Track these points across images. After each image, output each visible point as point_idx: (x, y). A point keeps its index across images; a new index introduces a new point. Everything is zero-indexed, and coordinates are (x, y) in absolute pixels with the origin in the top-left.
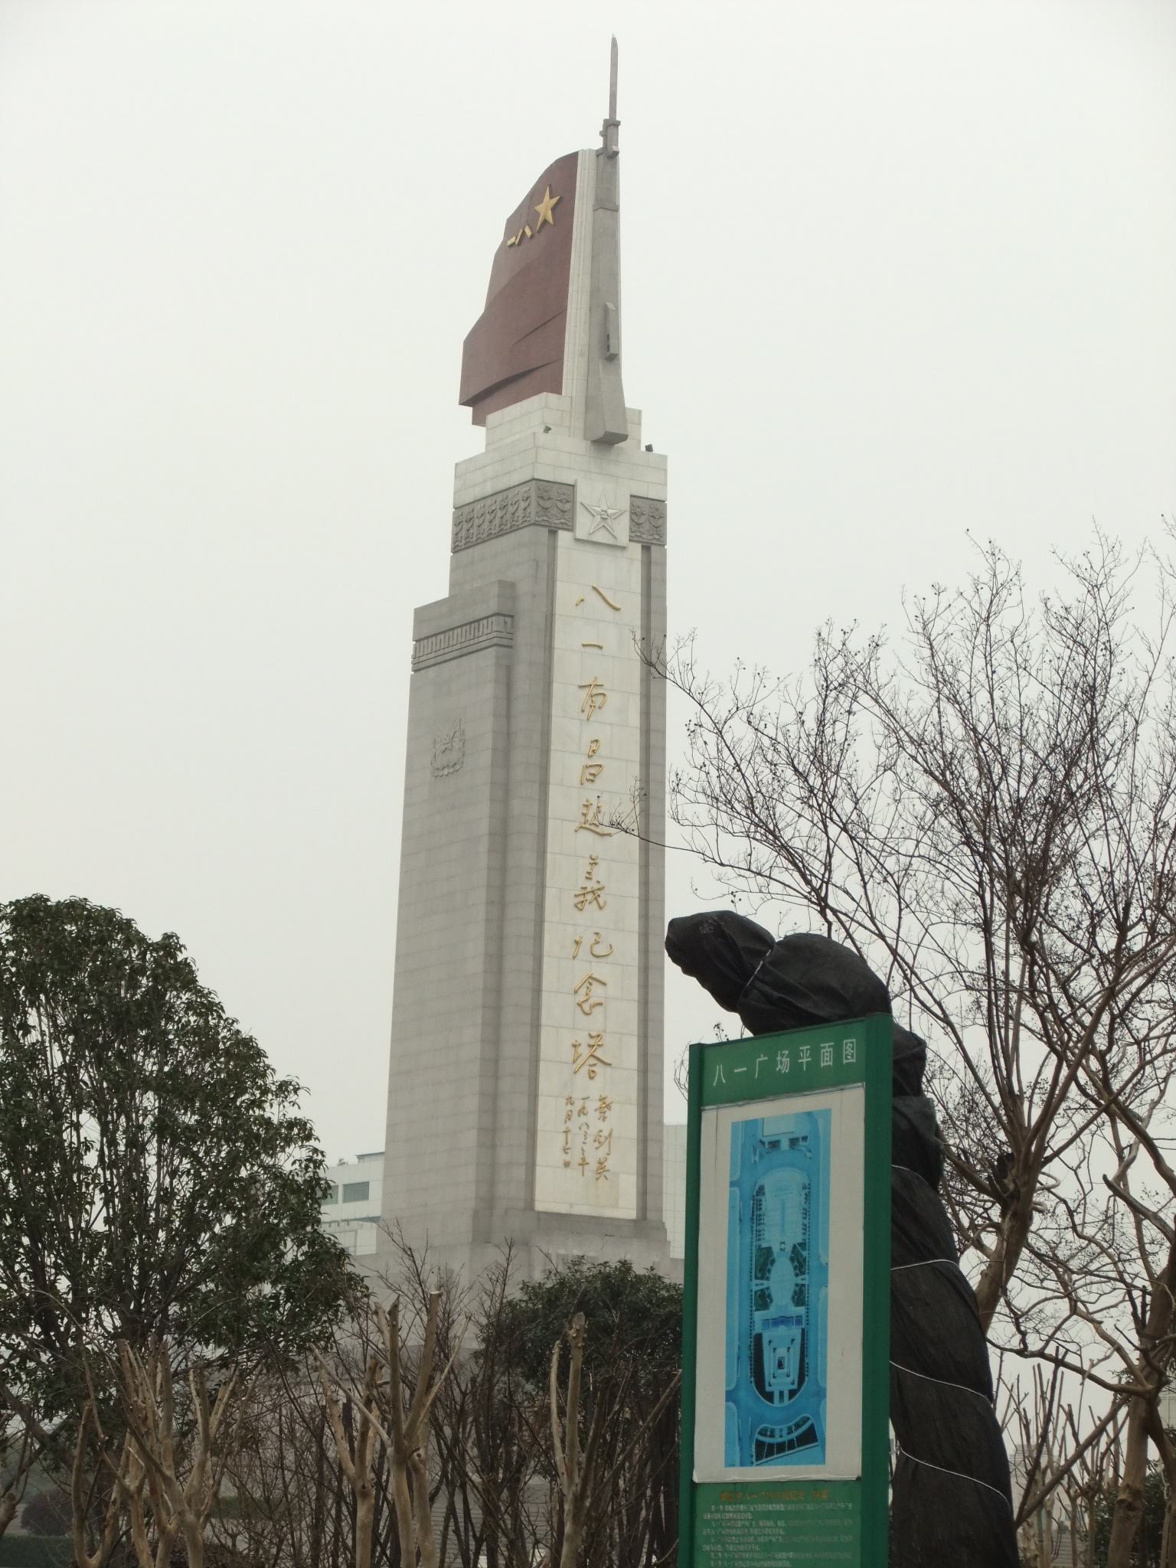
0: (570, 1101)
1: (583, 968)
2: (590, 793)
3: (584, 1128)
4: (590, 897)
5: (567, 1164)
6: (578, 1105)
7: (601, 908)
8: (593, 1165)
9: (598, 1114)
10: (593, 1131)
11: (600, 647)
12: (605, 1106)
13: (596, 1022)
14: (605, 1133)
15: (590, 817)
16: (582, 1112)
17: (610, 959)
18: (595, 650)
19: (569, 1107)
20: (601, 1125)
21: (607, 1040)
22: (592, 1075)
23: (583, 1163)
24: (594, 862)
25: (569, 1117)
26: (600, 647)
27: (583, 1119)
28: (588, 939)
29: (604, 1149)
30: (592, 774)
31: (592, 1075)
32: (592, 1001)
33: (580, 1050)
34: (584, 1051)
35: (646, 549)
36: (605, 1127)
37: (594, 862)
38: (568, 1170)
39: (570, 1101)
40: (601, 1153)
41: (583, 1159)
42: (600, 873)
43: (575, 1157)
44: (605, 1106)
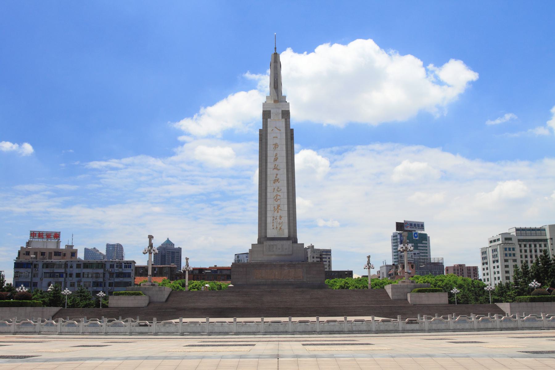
0: (273, 217)
1: (275, 194)
2: (276, 163)
12: (281, 217)
13: (278, 203)
16: (276, 219)
22: (278, 212)
24: (277, 175)
28: (276, 188)
30: (276, 160)
31: (278, 212)
34: (276, 208)
35: (286, 119)
36: (281, 221)
37: (277, 175)
39: (273, 217)
40: (280, 226)
42: (278, 176)
43: (275, 227)
44: (281, 217)
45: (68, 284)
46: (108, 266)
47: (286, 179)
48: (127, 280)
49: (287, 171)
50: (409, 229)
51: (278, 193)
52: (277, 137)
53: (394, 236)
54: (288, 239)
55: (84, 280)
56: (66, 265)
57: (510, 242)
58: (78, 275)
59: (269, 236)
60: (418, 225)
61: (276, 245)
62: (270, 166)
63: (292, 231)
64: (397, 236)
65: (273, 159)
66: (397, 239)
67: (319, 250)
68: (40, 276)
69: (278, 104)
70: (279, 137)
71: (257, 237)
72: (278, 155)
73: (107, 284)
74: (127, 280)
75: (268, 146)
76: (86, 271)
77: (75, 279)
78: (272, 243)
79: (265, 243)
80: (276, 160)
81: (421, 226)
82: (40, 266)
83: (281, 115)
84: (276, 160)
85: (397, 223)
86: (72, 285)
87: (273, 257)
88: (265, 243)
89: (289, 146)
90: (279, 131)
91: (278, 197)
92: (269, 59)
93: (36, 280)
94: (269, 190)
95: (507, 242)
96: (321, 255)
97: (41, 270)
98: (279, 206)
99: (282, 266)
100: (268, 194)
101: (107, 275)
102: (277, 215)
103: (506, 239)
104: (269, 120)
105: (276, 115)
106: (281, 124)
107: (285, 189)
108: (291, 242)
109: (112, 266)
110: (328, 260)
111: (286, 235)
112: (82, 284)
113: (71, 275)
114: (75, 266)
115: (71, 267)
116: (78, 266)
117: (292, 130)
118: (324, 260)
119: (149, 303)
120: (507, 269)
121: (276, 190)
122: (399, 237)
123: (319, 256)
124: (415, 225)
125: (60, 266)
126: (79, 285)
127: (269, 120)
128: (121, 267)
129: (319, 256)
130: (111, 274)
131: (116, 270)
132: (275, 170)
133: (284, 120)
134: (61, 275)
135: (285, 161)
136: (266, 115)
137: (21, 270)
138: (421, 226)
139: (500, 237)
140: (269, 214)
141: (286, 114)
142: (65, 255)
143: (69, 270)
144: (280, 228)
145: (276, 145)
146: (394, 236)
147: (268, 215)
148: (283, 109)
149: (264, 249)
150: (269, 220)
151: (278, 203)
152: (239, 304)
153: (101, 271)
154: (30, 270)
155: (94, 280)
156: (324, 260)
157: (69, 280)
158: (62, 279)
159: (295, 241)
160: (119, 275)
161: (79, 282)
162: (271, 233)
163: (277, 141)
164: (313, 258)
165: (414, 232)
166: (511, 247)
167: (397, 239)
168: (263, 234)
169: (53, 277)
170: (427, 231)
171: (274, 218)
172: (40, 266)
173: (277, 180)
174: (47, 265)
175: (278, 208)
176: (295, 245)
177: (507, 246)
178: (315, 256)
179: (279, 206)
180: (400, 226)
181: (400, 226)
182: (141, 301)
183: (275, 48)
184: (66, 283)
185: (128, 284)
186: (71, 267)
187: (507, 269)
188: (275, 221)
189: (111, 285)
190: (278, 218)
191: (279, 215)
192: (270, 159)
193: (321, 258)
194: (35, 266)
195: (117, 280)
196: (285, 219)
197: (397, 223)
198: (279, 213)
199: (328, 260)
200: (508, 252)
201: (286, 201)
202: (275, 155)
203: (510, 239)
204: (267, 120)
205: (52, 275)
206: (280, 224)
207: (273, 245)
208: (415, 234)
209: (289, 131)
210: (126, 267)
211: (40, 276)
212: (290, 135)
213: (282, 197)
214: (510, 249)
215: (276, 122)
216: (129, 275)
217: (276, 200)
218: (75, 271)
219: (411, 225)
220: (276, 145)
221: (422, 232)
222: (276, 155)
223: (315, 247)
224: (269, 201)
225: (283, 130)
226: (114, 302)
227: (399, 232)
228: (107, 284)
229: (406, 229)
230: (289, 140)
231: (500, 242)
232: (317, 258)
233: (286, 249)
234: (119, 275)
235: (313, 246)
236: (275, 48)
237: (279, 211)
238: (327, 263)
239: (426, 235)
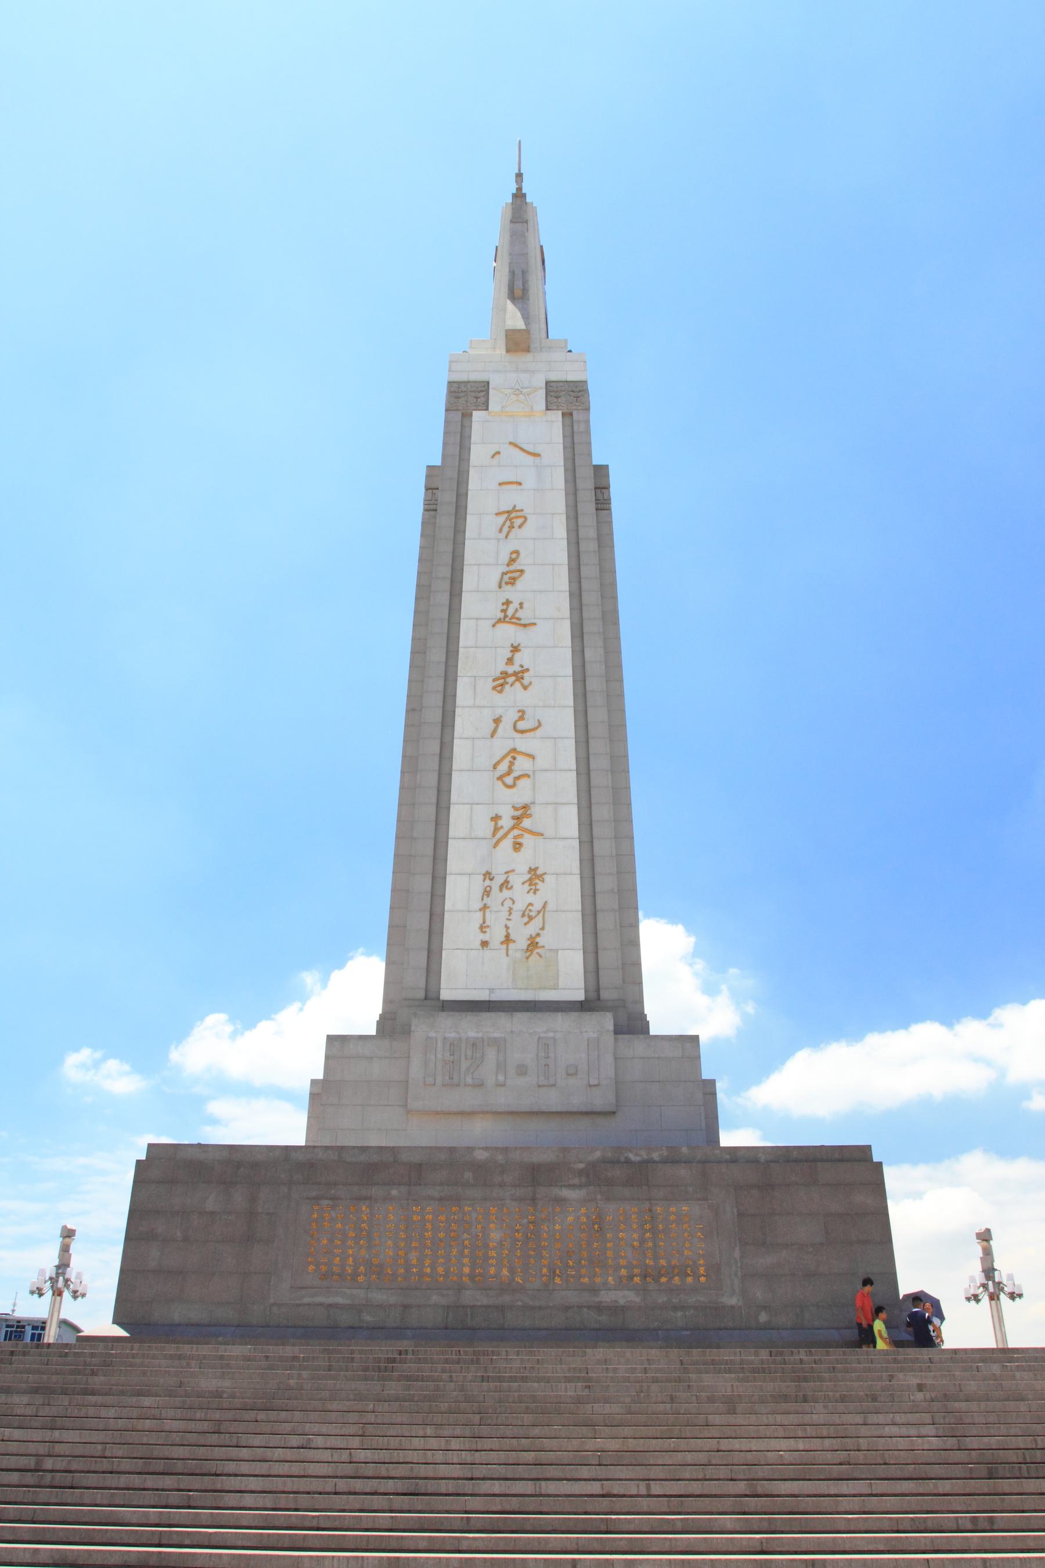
0: (488, 875)
1: (501, 746)
2: (509, 592)
3: (508, 903)
4: (511, 680)
5: (484, 944)
6: (499, 880)
7: (525, 688)
8: (522, 943)
9: (527, 887)
10: (520, 906)
11: (520, 484)
12: (535, 877)
13: (522, 793)
14: (538, 906)
15: (510, 613)
16: (505, 885)
17: (539, 733)
18: (514, 487)
19: (488, 882)
20: (530, 898)
21: (535, 810)
22: (517, 846)
23: (508, 940)
24: (515, 649)
25: (487, 892)
26: (520, 484)
27: (506, 893)
28: (511, 716)
29: (537, 922)
30: (511, 577)
31: (517, 846)
32: (516, 774)
33: (500, 823)
34: (506, 822)
35: (567, 415)
36: (537, 902)
37: (515, 649)
38: (487, 953)
39: (488, 875)
40: (533, 928)
41: (507, 936)
42: (523, 659)
43: (497, 934)
44: (535, 877)
47: (569, 671)
49: (579, 634)
51: (523, 744)
59: (446, 995)
61: (495, 1042)
62: (478, 603)
63: (609, 958)
65: (495, 575)
69: (529, 357)
70: (530, 481)
71: (376, 1009)
72: (522, 562)
75: (471, 522)
78: (470, 1028)
79: (421, 1030)
80: (512, 582)
83: (542, 393)
84: (511, 577)
88: (421, 1030)
89: (588, 532)
90: (530, 459)
91: (522, 764)
92: (492, 230)
94: (465, 723)
98: (523, 812)
99: (538, 1177)
100: (461, 751)
102: (504, 857)
104: (477, 415)
105: (518, 392)
106: (548, 431)
107: (562, 721)
108: (608, 1021)
117: (601, 472)
121: (506, 727)
127: (477, 415)
132: (508, 633)
133: (557, 416)
135: (563, 581)
136: (466, 398)
140: (462, 858)
141: (568, 398)
144: (533, 944)
145: (512, 519)
147: (453, 864)
148: (553, 377)
149: (416, 1070)
150: (460, 892)
151: (522, 793)
159: (632, 1023)
168: (415, 981)
173: (519, 676)
176: (637, 1047)
179: (523, 812)
183: (519, 176)
188: (497, 897)
190: (516, 880)
191: (522, 862)
196: (565, 891)
198: (527, 852)
201: (568, 784)
202: (504, 557)
204: (467, 416)
206: (528, 916)
207: (474, 1044)
209: (587, 484)
212: (591, 492)
213: (541, 762)
217: (507, 775)
222: (512, 561)
230: (587, 507)
233: (572, 1072)
236: (519, 176)
237: (527, 840)
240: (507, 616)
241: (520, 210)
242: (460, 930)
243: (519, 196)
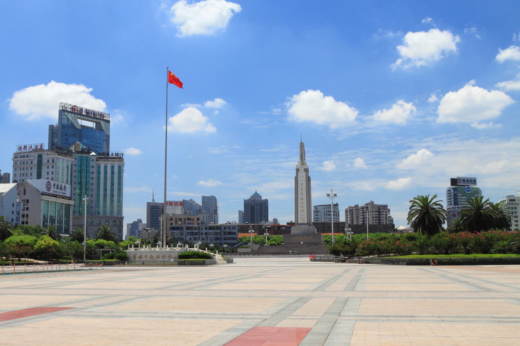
30: (302, 190)
45: (201, 239)
46: (223, 228)
48: (234, 236)
50: (462, 184)
52: (302, 180)
53: (448, 191)
54: (307, 224)
55: (210, 236)
56: (199, 228)
57: (514, 202)
58: (206, 234)
60: (471, 181)
62: (299, 193)
64: (450, 190)
66: (450, 193)
67: (377, 205)
68: (185, 234)
73: (223, 239)
74: (234, 236)
76: (210, 231)
77: (204, 236)
81: (474, 181)
82: (185, 229)
84: (302, 190)
85: (452, 179)
86: (203, 239)
87: (300, 232)
92: (299, 144)
93: (183, 237)
94: (299, 203)
95: (511, 202)
96: (379, 210)
97: (185, 231)
101: (223, 234)
102: (302, 214)
103: (511, 200)
106: (304, 174)
109: (225, 228)
110: (385, 213)
111: (306, 222)
112: (209, 239)
113: (202, 234)
114: (204, 228)
115: (202, 229)
116: (206, 228)
118: (381, 213)
119: (252, 251)
120: (516, 223)
122: (452, 191)
123: (377, 210)
124: (468, 181)
125: (196, 229)
126: (207, 240)
128: (230, 229)
129: (377, 210)
130: (225, 233)
131: (228, 230)
134: (196, 234)
136: (298, 170)
137: (174, 231)
138: (474, 181)
139: (506, 199)
140: (299, 214)
141: (307, 170)
142: (193, 220)
143: (201, 231)
145: (302, 184)
146: (449, 190)
150: (299, 216)
152: (284, 251)
153: (219, 231)
154: (179, 231)
155: (215, 236)
156: (381, 213)
157: (201, 237)
158: (197, 236)
160: (229, 233)
161: (207, 238)
162: (300, 221)
163: (302, 182)
164: (373, 212)
165: (466, 187)
166: (514, 206)
167: (450, 193)
169: (192, 235)
170: (479, 185)
171: (301, 215)
172: (185, 229)
174: (188, 228)
175: (303, 211)
177: (510, 206)
178: (374, 210)
180: (454, 182)
181: (454, 182)
182: (249, 250)
184: (199, 238)
185: (235, 239)
186: (202, 229)
187: (516, 223)
189: (225, 239)
192: (299, 190)
193: (379, 212)
194: (182, 229)
195: (228, 236)
197: (452, 179)
199: (385, 213)
200: (514, 210)
203: (514, 200)
205: (192, 234)
208: (467, 188)
210: (233, 229)
211: (185, 234)
214: (512, 208)
215: (302, 174)
216: (235, 233)
218: (204, 231)
219: (464, 180)
220: (302, 184)
221: (475, 187)
223: (375, 203)
224: (299, 208)
225: (305, 177)
226: (239, 250)
227: (452, 187)
228: (223, 239)
229: (459, 184)
231: (506, 203)
232: (376, 212)
234: (229, 233)
235: (373, 202)
238: (384, 216)
239: (478, 189)
240: (302, 194)
241: (302, 145)
242: (299, 219)
243: (301, 143)
